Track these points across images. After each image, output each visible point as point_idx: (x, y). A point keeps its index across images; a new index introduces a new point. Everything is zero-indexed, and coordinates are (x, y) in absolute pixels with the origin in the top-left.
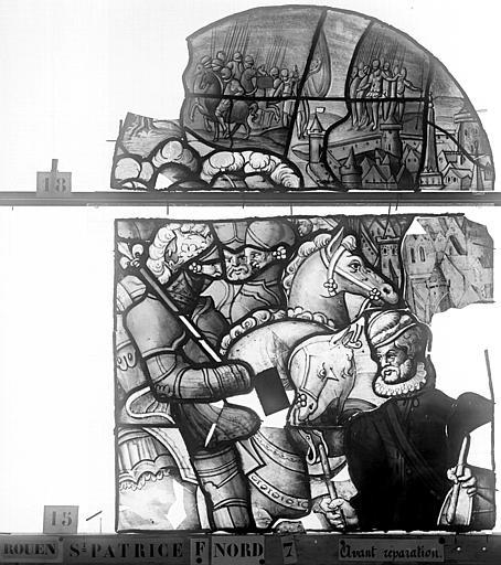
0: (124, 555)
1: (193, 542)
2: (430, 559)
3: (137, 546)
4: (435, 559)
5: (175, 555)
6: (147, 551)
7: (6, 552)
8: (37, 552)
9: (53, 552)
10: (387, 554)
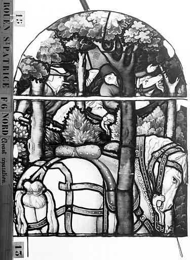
0: (4, 61)
2: (2, 179)
3: (8, 67)
5: (4, 84)
6: (6, 71)
10: (3, 160)
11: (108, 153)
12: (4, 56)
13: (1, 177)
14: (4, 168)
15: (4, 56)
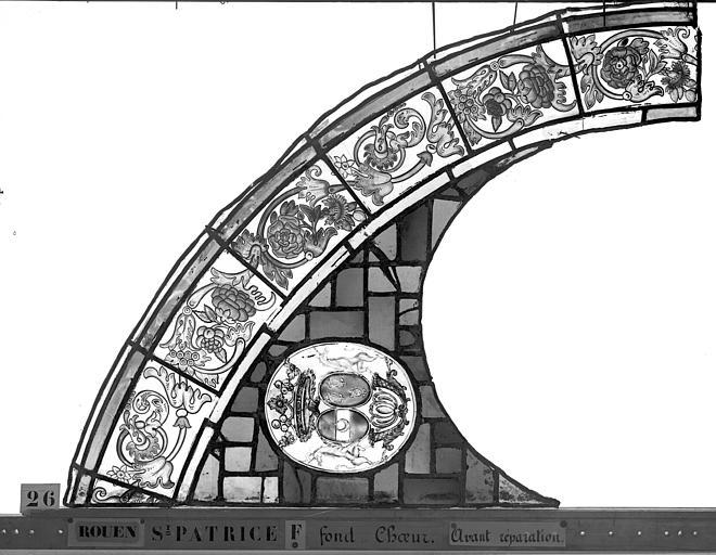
0: (212, 539)
1: (288, 525)
2: (551, 544)
3: (226, 528)
4: (555, 544)
5: (268, 539)
7: (82, 535)
8: (116, 535)
9: (133, 534)
11: (528, 151)
12: (199, 539)
13: (545, 544)
14: (523, 538)
15: (199, 539)
